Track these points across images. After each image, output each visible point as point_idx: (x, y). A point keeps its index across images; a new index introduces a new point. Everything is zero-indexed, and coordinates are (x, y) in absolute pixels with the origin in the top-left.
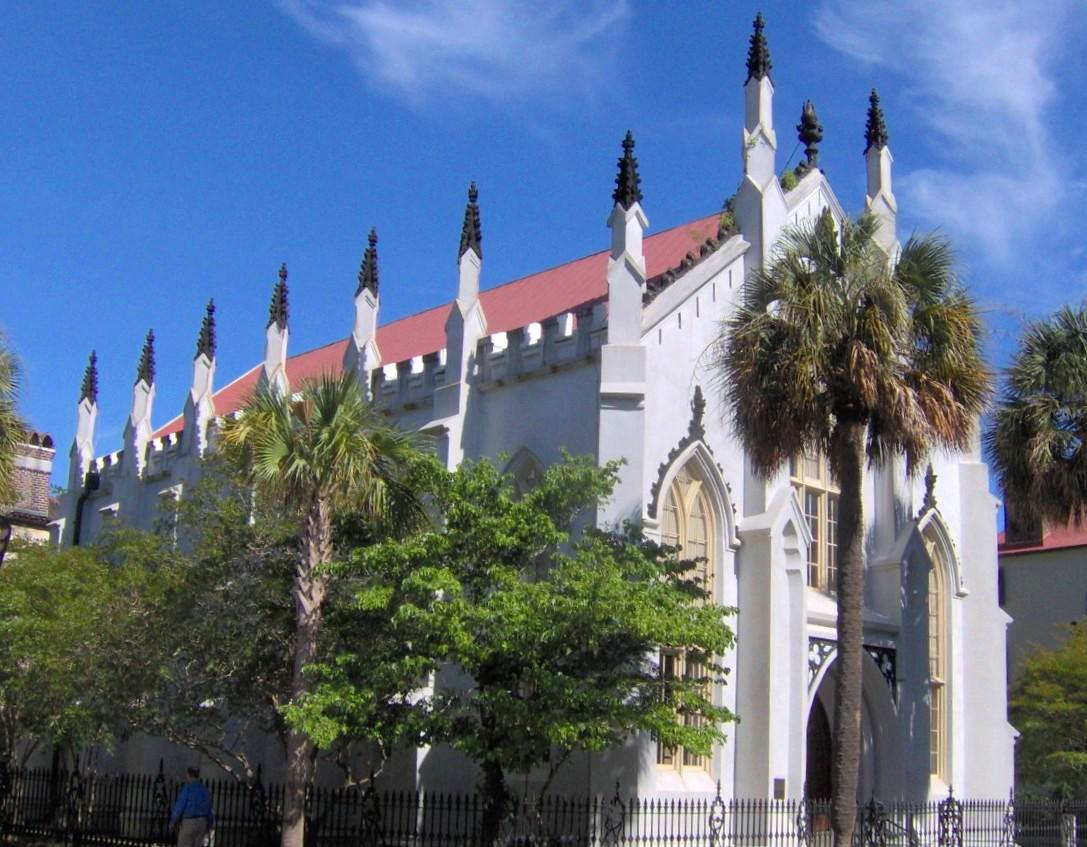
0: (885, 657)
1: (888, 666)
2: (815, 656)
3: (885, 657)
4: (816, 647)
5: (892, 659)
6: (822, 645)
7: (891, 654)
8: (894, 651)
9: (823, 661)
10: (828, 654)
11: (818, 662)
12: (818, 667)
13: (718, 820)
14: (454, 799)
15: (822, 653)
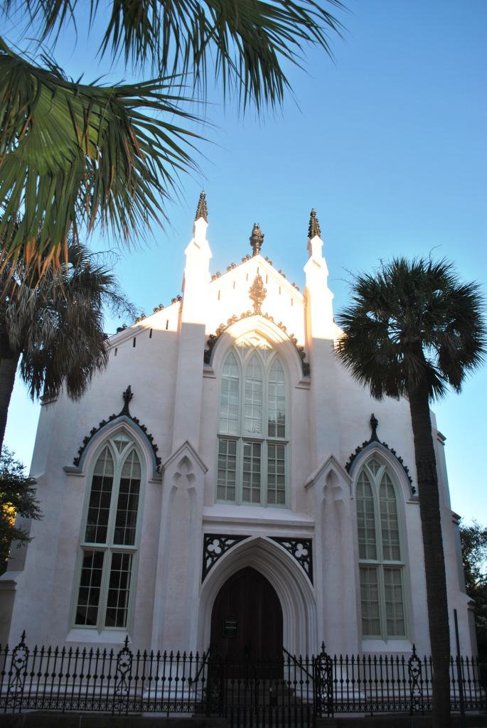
0: (300, 546)
1: (301, 551)
2: (215, 547)
3: (300, 546)
4: (216, 542)
5: (309, 549)
6: (223, 539)
7: (307, 543)
8: (310, 541)
9: (223, 552)
10: (230, 546)
11: (218, 551)
12: (219, 556)
13: (20, 661)
14: (356, 658)
15: (222, 545)
